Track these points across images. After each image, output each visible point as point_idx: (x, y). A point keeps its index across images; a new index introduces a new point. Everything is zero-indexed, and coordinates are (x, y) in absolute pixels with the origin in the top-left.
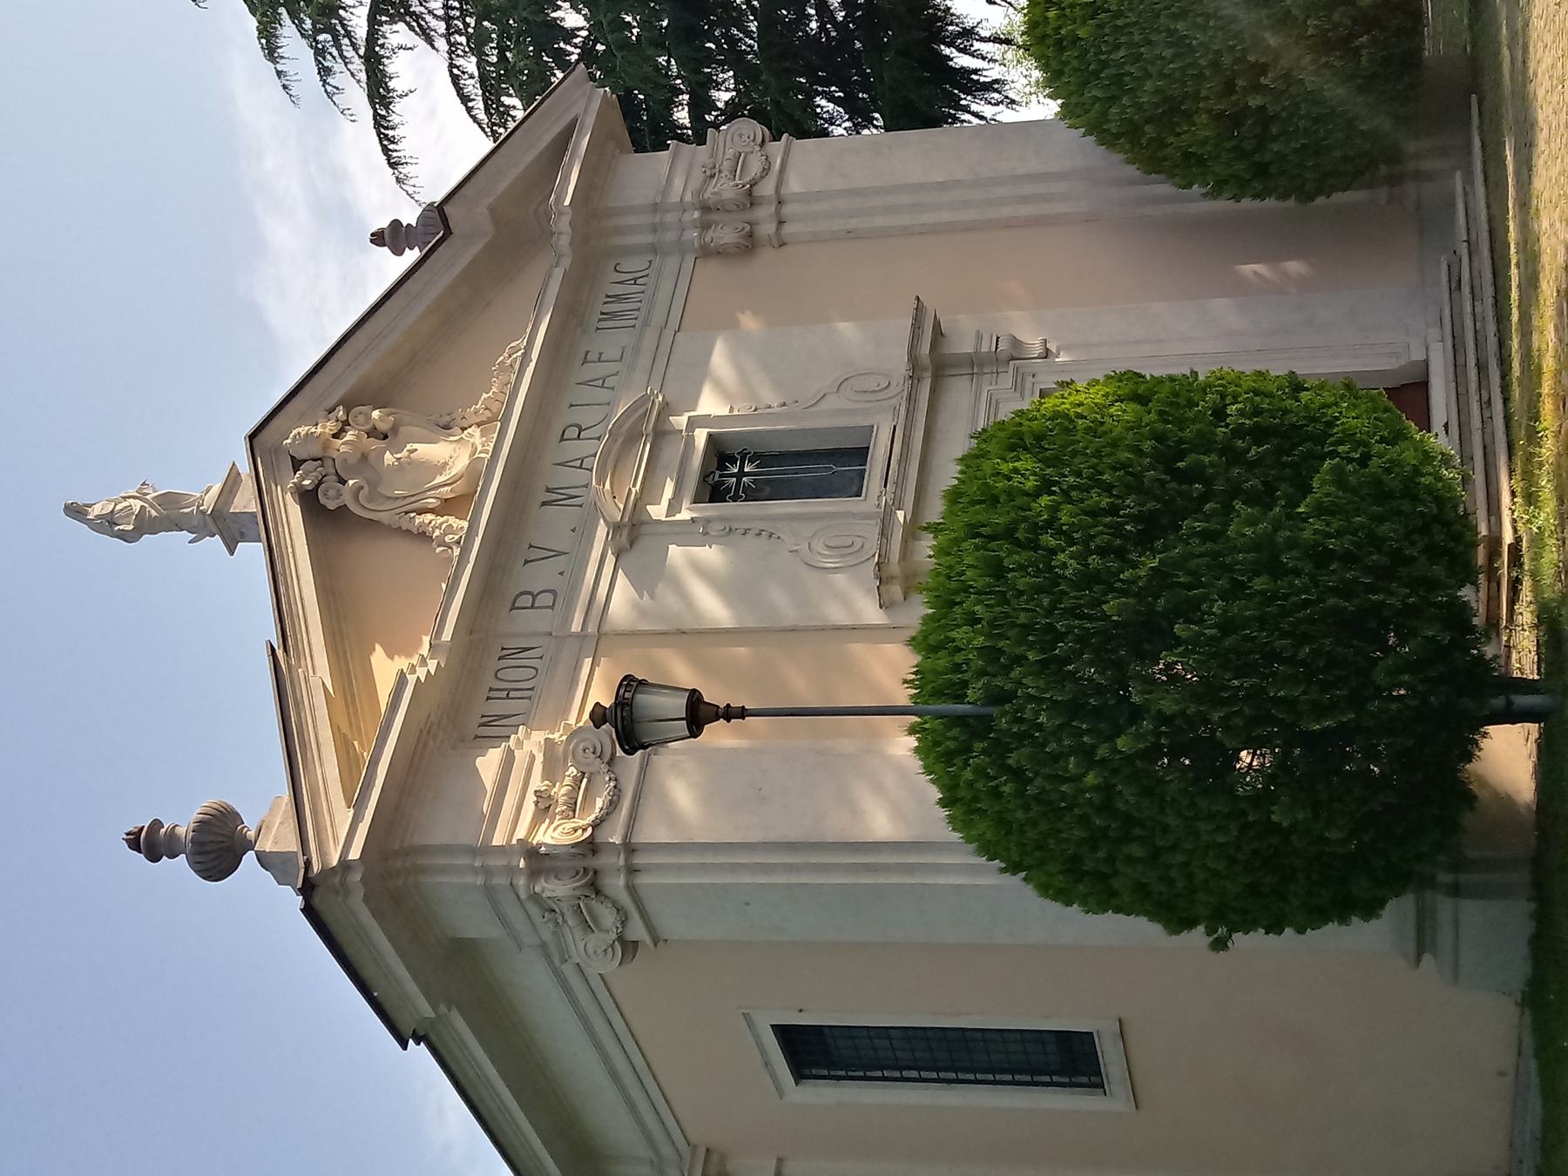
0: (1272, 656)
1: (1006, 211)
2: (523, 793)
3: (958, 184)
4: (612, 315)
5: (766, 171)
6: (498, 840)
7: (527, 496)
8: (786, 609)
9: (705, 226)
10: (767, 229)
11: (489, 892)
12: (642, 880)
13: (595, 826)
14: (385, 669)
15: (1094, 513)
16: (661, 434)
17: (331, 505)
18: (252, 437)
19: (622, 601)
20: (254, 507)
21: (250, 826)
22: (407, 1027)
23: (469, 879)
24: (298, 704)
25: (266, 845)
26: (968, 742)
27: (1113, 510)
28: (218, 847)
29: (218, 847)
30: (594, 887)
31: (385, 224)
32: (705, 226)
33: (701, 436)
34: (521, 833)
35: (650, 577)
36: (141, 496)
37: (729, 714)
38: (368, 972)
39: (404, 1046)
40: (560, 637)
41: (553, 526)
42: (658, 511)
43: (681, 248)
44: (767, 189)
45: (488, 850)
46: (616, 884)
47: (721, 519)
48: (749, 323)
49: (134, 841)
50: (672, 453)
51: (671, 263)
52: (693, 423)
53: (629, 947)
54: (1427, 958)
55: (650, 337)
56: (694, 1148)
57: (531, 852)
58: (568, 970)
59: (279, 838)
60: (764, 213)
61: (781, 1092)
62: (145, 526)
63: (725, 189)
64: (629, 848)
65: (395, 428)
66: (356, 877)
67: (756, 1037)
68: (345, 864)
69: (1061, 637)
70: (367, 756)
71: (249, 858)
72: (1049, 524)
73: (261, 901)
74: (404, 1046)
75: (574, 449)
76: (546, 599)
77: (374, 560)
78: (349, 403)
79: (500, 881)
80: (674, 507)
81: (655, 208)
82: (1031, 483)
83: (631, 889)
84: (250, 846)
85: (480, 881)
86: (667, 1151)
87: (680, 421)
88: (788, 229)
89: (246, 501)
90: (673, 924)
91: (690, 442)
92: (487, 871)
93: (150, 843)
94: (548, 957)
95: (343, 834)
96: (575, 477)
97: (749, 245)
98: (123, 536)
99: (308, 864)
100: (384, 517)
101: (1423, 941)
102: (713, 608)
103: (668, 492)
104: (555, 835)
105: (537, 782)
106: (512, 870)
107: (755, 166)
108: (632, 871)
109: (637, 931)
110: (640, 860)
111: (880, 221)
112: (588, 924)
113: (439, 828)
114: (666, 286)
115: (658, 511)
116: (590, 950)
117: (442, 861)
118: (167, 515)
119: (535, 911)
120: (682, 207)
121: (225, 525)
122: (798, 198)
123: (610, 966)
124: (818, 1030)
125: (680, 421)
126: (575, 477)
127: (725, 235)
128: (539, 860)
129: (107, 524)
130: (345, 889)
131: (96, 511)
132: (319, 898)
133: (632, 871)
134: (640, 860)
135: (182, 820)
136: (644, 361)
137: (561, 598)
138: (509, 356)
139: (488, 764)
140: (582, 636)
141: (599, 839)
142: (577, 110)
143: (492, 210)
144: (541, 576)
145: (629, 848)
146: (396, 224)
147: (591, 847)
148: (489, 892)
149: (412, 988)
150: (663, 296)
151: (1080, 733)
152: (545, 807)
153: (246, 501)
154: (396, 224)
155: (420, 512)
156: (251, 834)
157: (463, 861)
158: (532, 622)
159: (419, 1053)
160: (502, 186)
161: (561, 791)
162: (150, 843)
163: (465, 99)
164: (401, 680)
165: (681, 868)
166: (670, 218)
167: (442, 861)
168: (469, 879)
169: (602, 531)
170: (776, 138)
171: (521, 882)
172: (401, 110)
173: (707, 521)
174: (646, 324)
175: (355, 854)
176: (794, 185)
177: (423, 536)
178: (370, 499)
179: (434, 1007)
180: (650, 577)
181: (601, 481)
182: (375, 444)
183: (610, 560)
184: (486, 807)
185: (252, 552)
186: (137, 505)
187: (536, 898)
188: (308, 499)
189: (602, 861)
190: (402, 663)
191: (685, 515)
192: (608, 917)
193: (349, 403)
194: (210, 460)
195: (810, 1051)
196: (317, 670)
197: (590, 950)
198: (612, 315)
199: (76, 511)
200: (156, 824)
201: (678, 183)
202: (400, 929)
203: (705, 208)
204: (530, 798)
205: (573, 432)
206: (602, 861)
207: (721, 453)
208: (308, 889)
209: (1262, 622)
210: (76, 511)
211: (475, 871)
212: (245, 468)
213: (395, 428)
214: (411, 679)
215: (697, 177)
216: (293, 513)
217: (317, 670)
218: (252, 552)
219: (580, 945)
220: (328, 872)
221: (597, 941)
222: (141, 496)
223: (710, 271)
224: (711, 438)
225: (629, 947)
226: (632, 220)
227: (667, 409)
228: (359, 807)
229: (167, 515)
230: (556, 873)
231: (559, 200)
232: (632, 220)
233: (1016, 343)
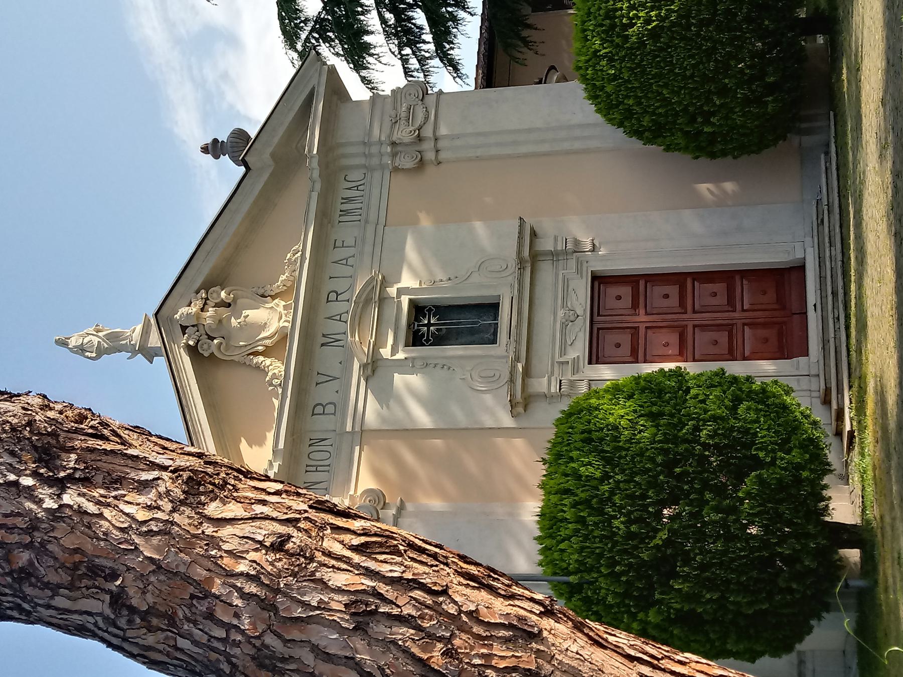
0: (728, 582)
1: (566, 146)
3: (539, 129)
4: (345, 213)
5: (427, 118)
7: (313, 339)
8: (462, 421)
9: (394, 155)
10: (430, 156)
16: (383, 299)
19: (372, 412)
31: (209, 140)
32: (394, 155)
33: (405, 300)
35: (386, 395)
41: (328, 359)
42: (386, 352)
44: (428, 132)
47: (423, 358)
48: (425, 222)
50: (390, 312)
51: (377, 175)
52: (400, 292)
55: (370, 229)
60: (428, 146)
62: (101, 352)
65: (235, 300)
75: (337, 308)
76: (330, 409)
77: (232, 381)
78: (207, 286)
80: (394, 351)
87: (392, 291)
88: (443, 156)
89: (154, 340)
91: (400, 303)
96: (337, 327)
97: (421, 164)
100: (236, 358)
102: (422, 417)
103: (390, 341)
111: (494, 151)
114: (376, 192)
115: (386, 352)
118: (114, 344)
125: (392, 291)
126: (337, 327)
127: (407, 162)
131: (73, 342)
136: (368, 248)
137: (339, 407)
140: (353, 432)
142: (314, 82)
143: (273, 155)
144: (325, 393)
146: (215, 141)
150: (374, 202)
151: (629, 606)
154: (215, 141)
155: (256, 354)
158: (322, 424)
160: (276, 140)
166: (374, 150)
169: (356, 366)
173: (414, 359)
176: (443, 131)
177: (258, 367)
178: (227, 349)
180: (386, 395)
181: (353, 335)
182: (224, 312)
183: (363, 382)
186: (96, 340)
188: (193, 351)
191: (401, 355)
193: (207, 286)
198: (345, 213)
201: (376, 132)
203: (394, 144)
205: (333, 296)
207: (418, 309)
209: (721, 565)
213: (235, 300)
215: (387, 124)
223: (400, 180)
224: (411, 300)
227: (385, 283)
229: (114, 344)
231: (310, 151)
233: (577, 242)
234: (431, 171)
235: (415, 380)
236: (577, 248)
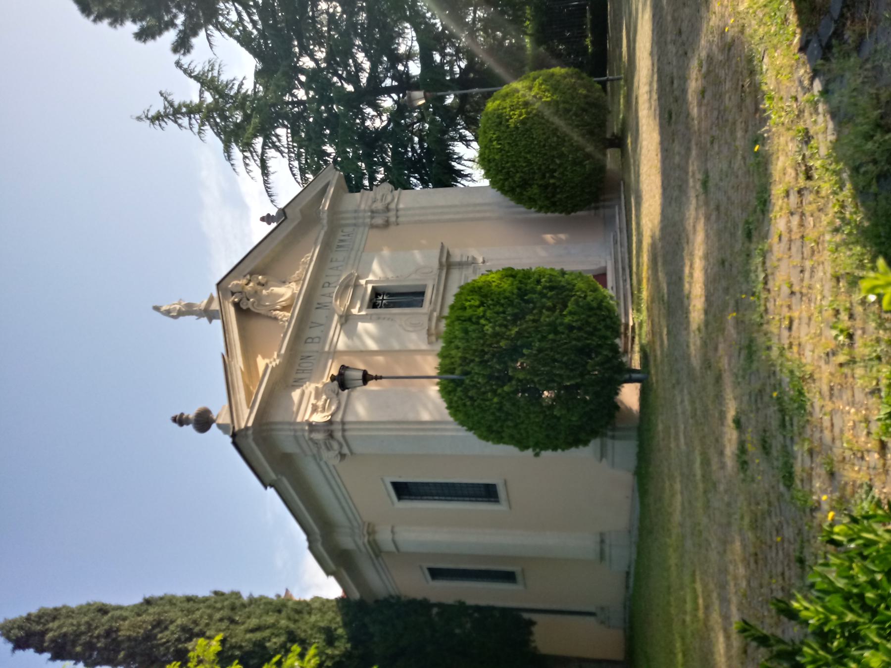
0: (555, 360)
2: (309, 405)
5: (393, 200)
6: (299, 419)
7: (311, 307)
8: (396, 346)
9: (372, 218)
10: (393, 219)
11: (296, 438)
12: (348, 434)
13: (332, 415)
14: (261, 363)
15: (498, 313)
16: (356, 286)
17: (244, 307)
18: (218, 284)
19: (342, 343)
20: (218, 308)
21: (214, 414)
22: (267, 481)
23: (289, 433)
24: (232, 374)
25: (220, 421)
26: (457, 389)
27: (504, 312)
28: (203, 422)
29: (203, 422)
30: (331, 435)
32: (372, 218)
33: (370, 287)
34: (306, 418)
35: (352, 334)
36: (179, 304)
37: (377, 378)
38: (254, 464)
39: (266, 488)
40: (321, 352)
41: (319, 316)
42: (355, 311)
43: (364, 225)
44: (393, 206)
45: (295, 423)
46: (338, 435)
47: (376, 314)
49: (175, 420)
50: (360, 293)
51: (361, 229)
52: (367, 282)
53: (343, 456)
54: (604, 460)
55: (353, 253)
56: (364, 523)
57: (310, 424)
58: (322, 463)
59: (224, 419)
60: (392, 214)
61: (393, 503)
62: (181, 313)
63: (379, 206)
64: (343, 423)
65: (267, 283)
66: (250, 432)
67: (385, 485)
68: (247, 428)
69: (486, 353)
70: (255, 392)
71: (214, 426)
72: (483, 316)
73: (218, 440)
74: (266, 488)
75: (327, 290)
76: (317, 340)
77: (258, 326)
78: (251, 274)
79: (299, 434)
80: (360, 310)
81: (356, 211)
82: (477, 303)
83: (344, 437)
84: (213, 421)
85: (292, 433)
86: (355, 524)
87: (363, 282)
88: (401, 219)
89: (215, 306)
90: (357, 448)
91: (366, 289)
92: (295, 431)
93: (180, 421)
94: (315, 459)
95: (246, 418)
96: (327, 300)
97: (387, 224)
98: (173, 317)
99: (234, 428)
100: (262, 312)
101: (603, 455)
102: (372, 345)
103: (358, 306)
104: (319, 418)
105: (313, 401)
106: (303, 430)
107: (389, 198)
108: (344, 430)
109: (345, 450)
110: (347, 427)
112: (329, 448)
113: (278, 416)
115: (355, 311)
116: (330, 457)
117: (279, 427)
118: (188, 310)
119: (310, 443)
120: (365, 211)
121: (208, 314)
122: (403, 209)
123: (336, 461)
124: (406, 484)
125: (363, 282)
126: (327, 300)
127: (379, 221)
128: (313, 427)
129: (168, 313)
130: (246, 436)
131: (164, 308)
132: (237, 438)
133: (344, 430)
134: (347, 427)
135: (191, 413)
137: (322, 339)
138: (306, 258)
139: (296, 395)
140: (329, 353)
141: (334, 419)
143: (301, 211)
144: (315, 332)
145: (343, 423)
147: (330, 422)
148: (296, 438)
149: (268, 469)
151: (492, 385)
152: (315, 409)
153: (215, 306)
155: (275, 310)
156: (215, 417)
157: (286, 427)
159: (271, 491)
160: (304, 203)
161: (320, 403)
162: (180, 421)
164: (267, 366)
165: (360, 430)
166: (361, 214)
167: (279, 427)
168: (289, 433)
169: (336, 318)
170: (396, 189)
171: (306, 434)
173: (371, 315)
174: (352, 249)
175: (250, 424)
177: (275, 318)
179: (277, 475)
180: (352, 334)
181: (336, 300)
182: (259, 288)
183: (339, 327)
184: (295, 409)
185: (217, 323)
187: (311, 439)
188: (237, 305)
189: (334, 427)
190: (267, 361)
191: (363, 313)
192: (335, 445)
193: (251, 274)
194: (203, 292)
195: (403, 490)
196: (238, 362)
197: (330, 457)
198: (339, 246)
199: (157, 309)
200: (182, 414)
202: (267, 449)
203: (372, 212)
204: (310, 407)
205: (327, 285)
206: (334, 427)
207: (376, 293)
208: (234, 436)
209: (552, 349)
210: (157, 309)
211: (290, 430)
212: (215, 295)
213: (267, 283)
214: (270, 366)
216: (231, 311)
217: (238, 362)
218: (217, 323)
219: (326, 455)
220: (241, 430)
221: (332, 454)
222: (179, 304)
223: (375, 233)
224: (373, 288)
225: (343, 456)
226: (349, 215)
227: (358, 278)
228: (252, 408)
229: (188, 310)
230: (318, 431)
231: (324, 207)
232: (349, 215)
233: (474, 258)
234: (392, 228)
235: (370, 327)
236: (474, 261)
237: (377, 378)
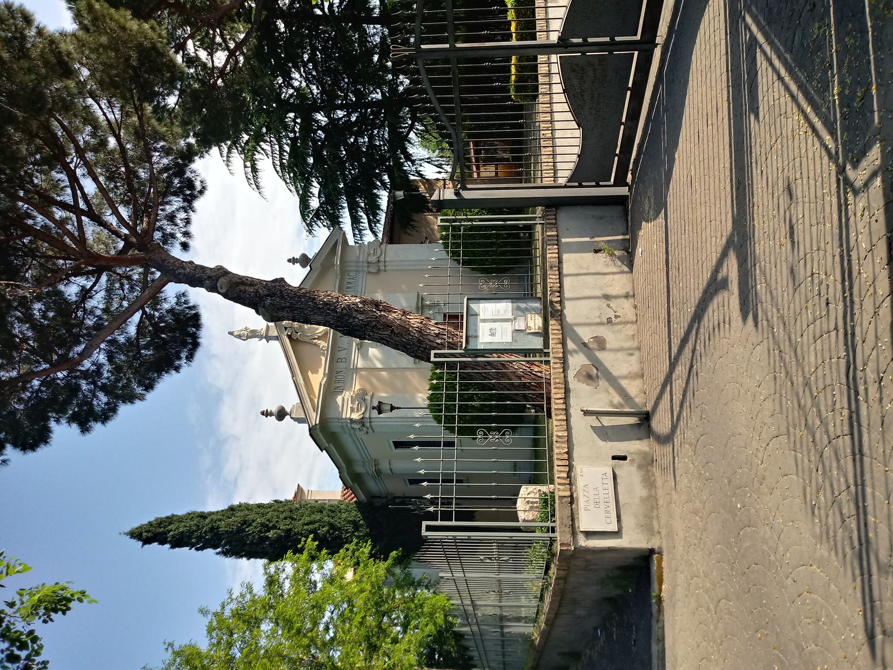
4: (348, 288)
9: (368, 267)
32: (368, 267)
37: (398, 408)
40: (348, 369)
43: (363, 271)
44: (382, 259)
51: (361, 274)
57: (351, 420)
64: (370, 418)
71: (288, 417)
104: (356, 416)
105: (350, 405)
113: (331, 414)
114: (360, 280)
127: (374, 270)
137: (347, 359)
145: (370, 418)
150: (360, 284)
152: (352, 410)
161: (355, 406)
163: (277, 172)
172: (260, 174)
198: (348, 288)
223: (370, 277)
226: (352, 264)
232: (352, 264)
234: (382, 274)
237: (398, 408)
